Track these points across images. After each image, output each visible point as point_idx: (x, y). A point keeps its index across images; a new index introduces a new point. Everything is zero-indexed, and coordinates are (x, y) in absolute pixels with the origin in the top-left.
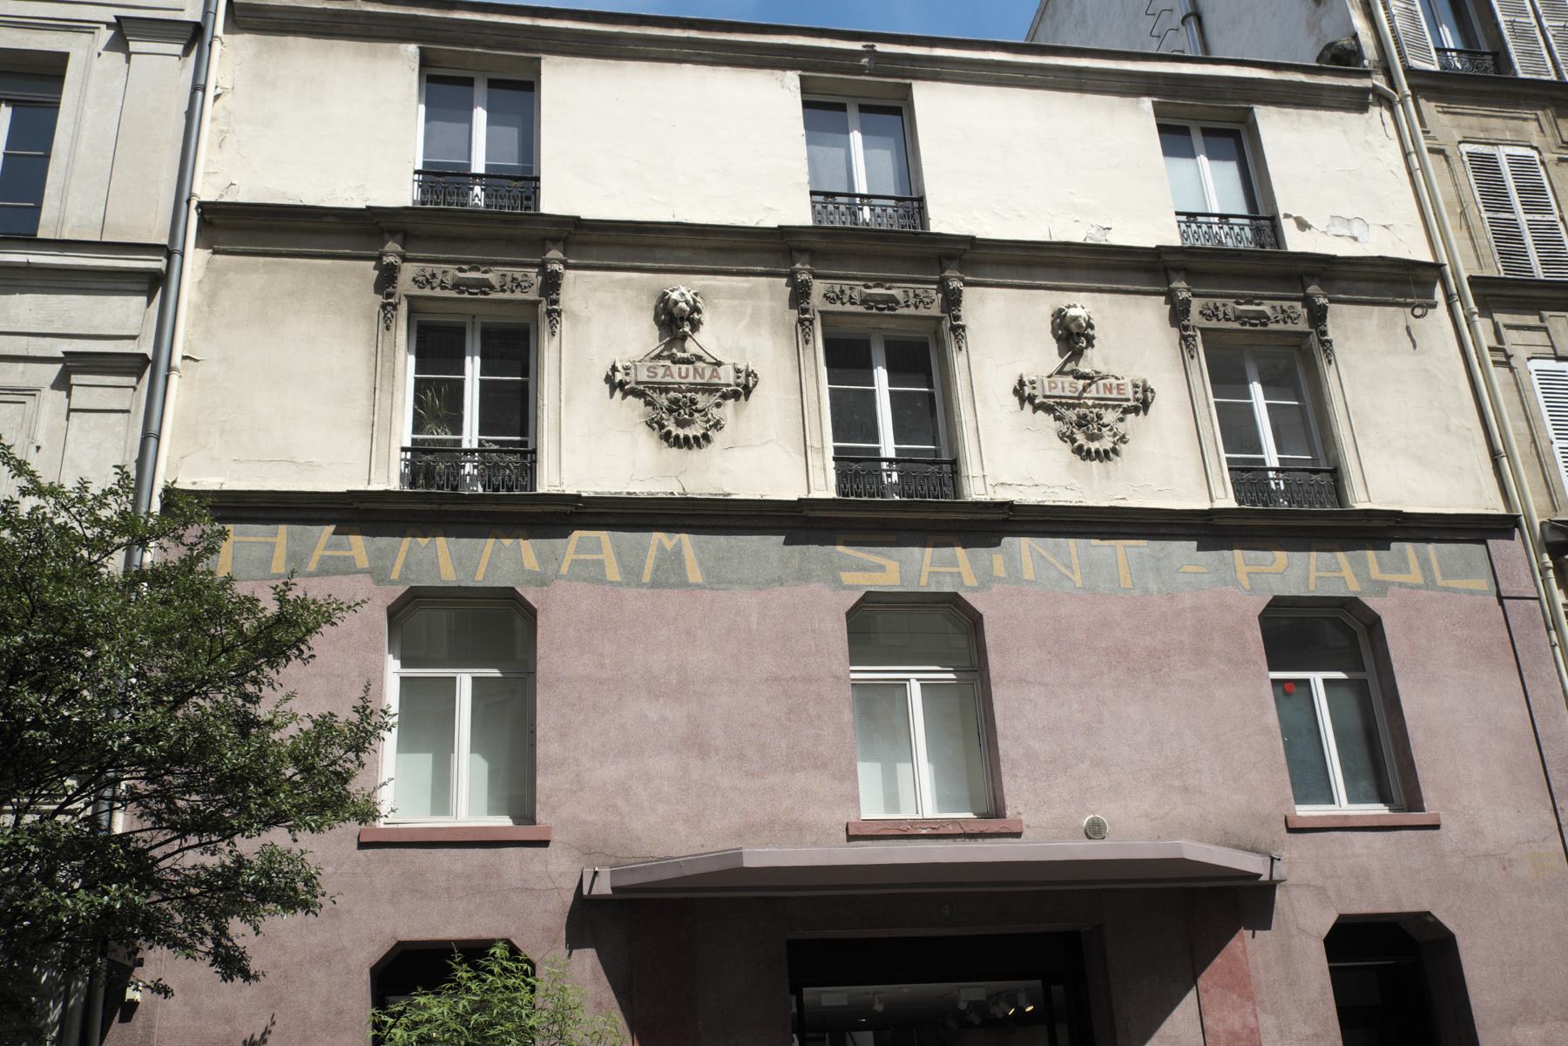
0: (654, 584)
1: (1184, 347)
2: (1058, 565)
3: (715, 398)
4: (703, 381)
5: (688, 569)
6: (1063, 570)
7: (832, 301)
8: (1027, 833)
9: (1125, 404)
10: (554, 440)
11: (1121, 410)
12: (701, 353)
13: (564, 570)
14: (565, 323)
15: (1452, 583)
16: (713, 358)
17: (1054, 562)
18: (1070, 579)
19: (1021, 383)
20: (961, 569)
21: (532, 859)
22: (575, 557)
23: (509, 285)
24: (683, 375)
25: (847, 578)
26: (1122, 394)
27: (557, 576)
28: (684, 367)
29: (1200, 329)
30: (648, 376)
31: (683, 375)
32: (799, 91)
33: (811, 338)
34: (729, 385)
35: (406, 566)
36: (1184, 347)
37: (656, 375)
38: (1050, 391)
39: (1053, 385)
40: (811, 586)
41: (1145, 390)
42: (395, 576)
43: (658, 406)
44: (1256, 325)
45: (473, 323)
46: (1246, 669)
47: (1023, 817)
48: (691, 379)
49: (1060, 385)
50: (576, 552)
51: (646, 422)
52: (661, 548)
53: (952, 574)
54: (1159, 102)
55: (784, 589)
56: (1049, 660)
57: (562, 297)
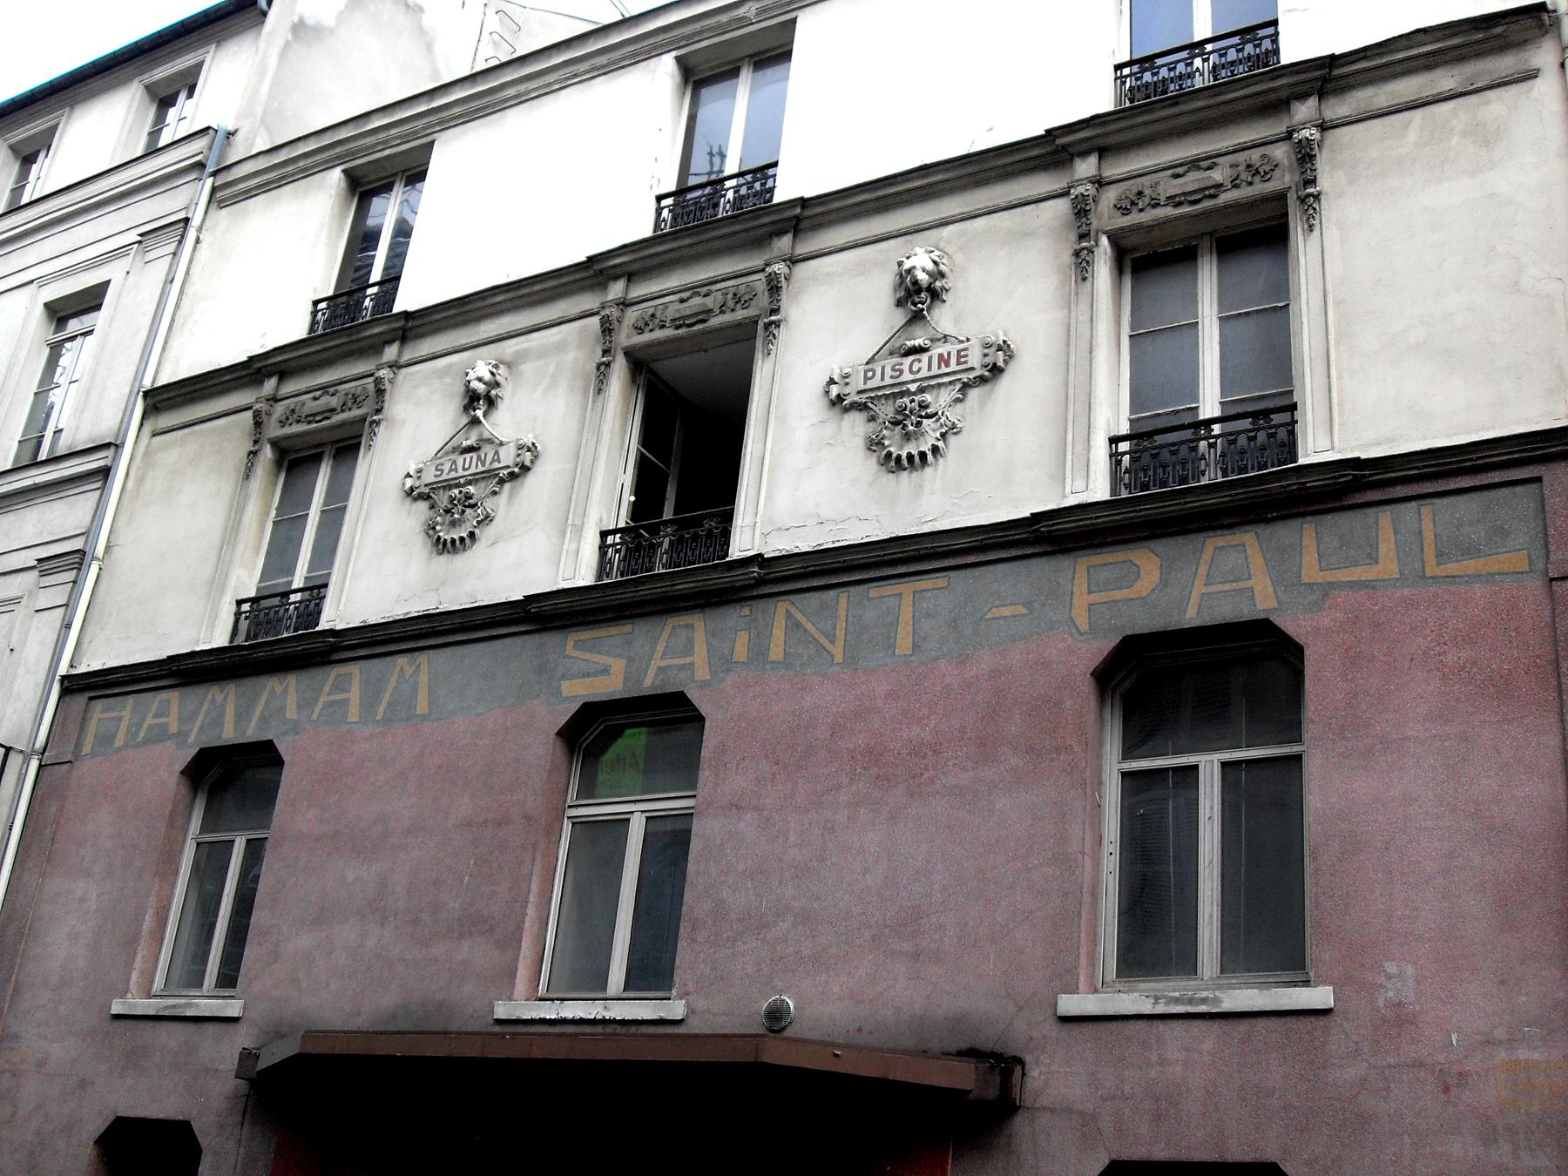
3: (492, 485)
9: (964, 377)
11: (958, 386)
15: (1451, 568)
24: (467, 466)
26: (966, 362)
28: (468, 456)
37: (442, 471)
46: (1052, 760)
48: (473, 470)
56: (774, 774)
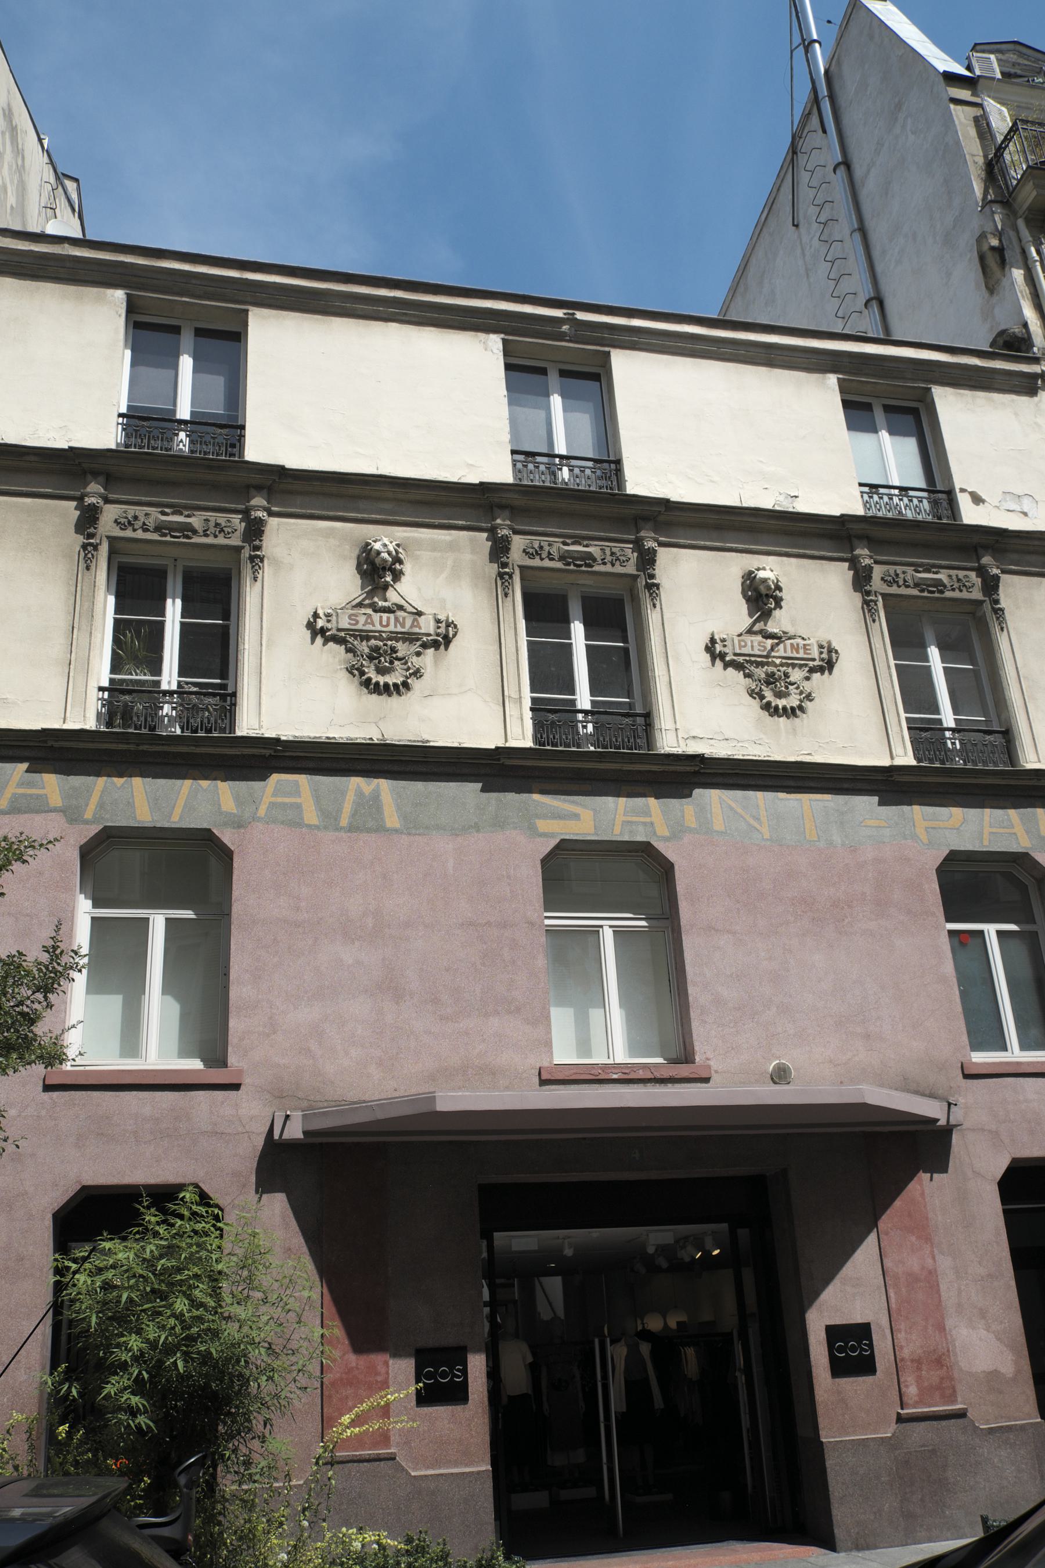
0: (352, 828)
1: (866, 611)
2: (748, 817)
3: (416, 647)
4: (403, 630)
5: (386, 814)
6: (752, 822)
7: (531, 556)
8: (715, 1078)
9: (811, 664)
10: (254, 682)
11: (807, 669)
12: (402, 602)
13: (262, 812)
14: (268, 571)
16: (414, 607)
17: (743, 813)
18: (758, 830)
19: (713, 641)
20: (654, 819)
21: (223, 1103)
22: (273, 799)
23: (212, 530)
24: (384, 623)
25: (543, 825)
26: (810, 654)
27: (255, 818)
28: (385, 616)
29: (881, 594)
30: (349, 624)
31: (384, 623)
32: (502, 353)
33: (510, 591)
34: (429, 635)
35: (101, 805)
36: (866, 611)
37: (357, 622)
38: (740, 649)
39: (743, 644)
40: (508, 833)
41: (831, 650)
42: (88, 815)
43: (359, 653)
44: (933, 592)
45: (175, 566)
46: (924, 920)
47: (711, 1063)
48: (391, 628)
49: (749, 644)
50: (274, 795)
51: (347, 668)
52: (360, 793)
53: (645, 824)
54: (844, 379)
55: (481, 835)
56: (738, 909)
57: (264, 544)
